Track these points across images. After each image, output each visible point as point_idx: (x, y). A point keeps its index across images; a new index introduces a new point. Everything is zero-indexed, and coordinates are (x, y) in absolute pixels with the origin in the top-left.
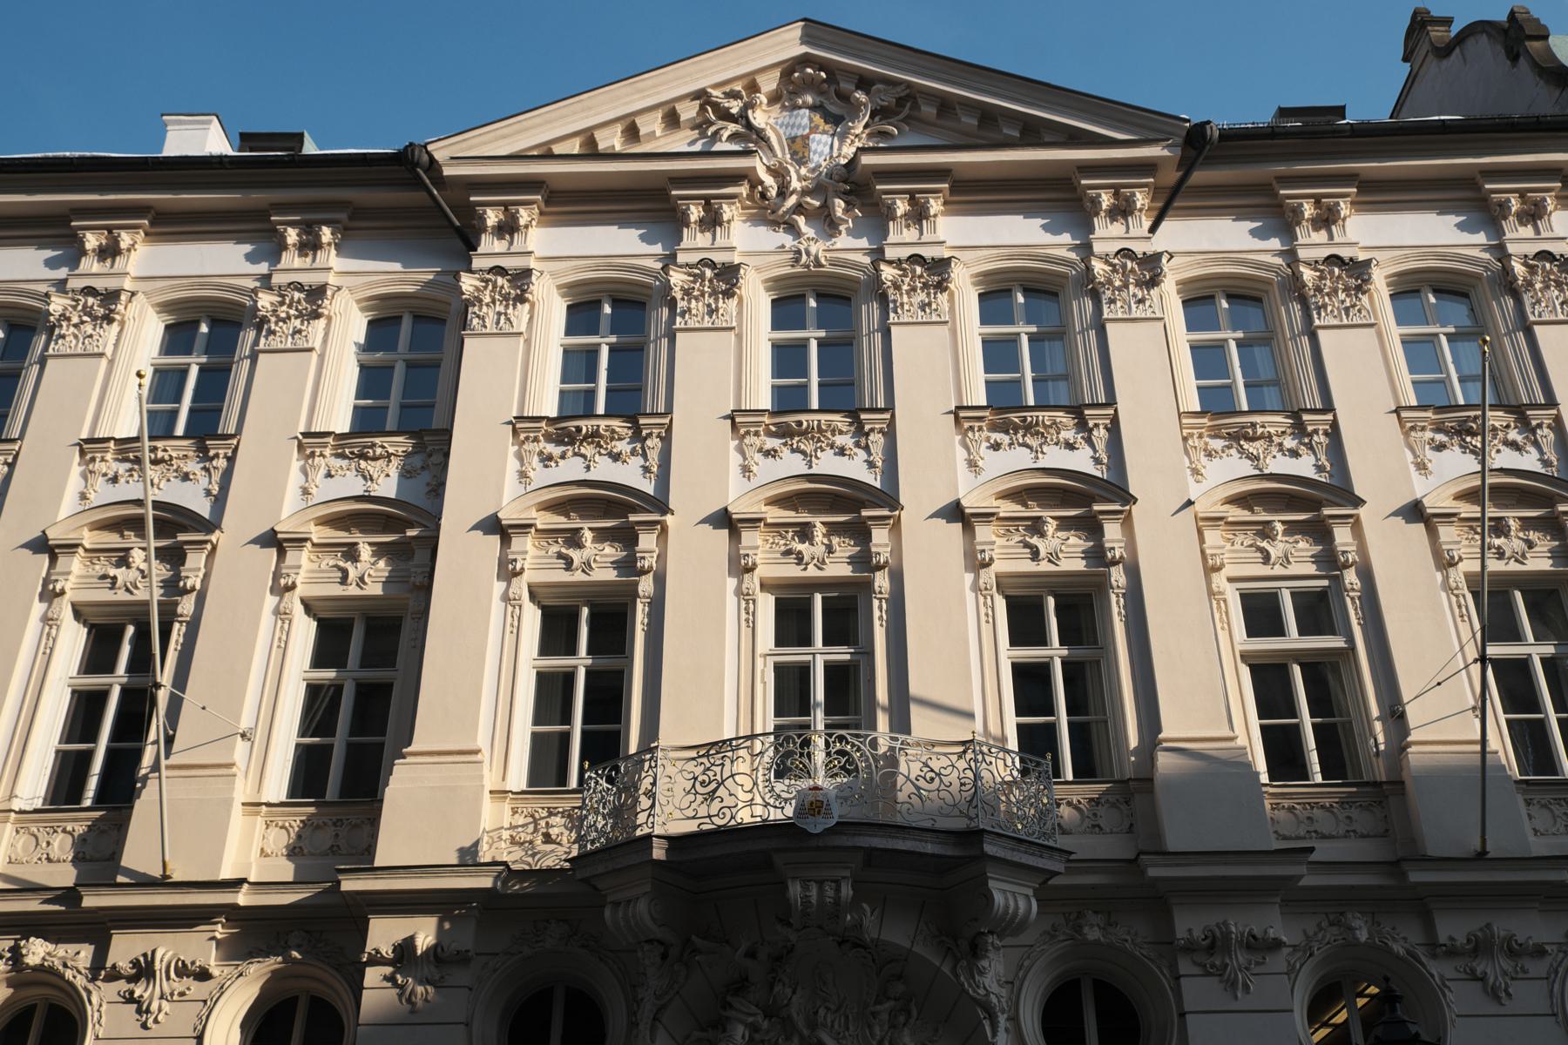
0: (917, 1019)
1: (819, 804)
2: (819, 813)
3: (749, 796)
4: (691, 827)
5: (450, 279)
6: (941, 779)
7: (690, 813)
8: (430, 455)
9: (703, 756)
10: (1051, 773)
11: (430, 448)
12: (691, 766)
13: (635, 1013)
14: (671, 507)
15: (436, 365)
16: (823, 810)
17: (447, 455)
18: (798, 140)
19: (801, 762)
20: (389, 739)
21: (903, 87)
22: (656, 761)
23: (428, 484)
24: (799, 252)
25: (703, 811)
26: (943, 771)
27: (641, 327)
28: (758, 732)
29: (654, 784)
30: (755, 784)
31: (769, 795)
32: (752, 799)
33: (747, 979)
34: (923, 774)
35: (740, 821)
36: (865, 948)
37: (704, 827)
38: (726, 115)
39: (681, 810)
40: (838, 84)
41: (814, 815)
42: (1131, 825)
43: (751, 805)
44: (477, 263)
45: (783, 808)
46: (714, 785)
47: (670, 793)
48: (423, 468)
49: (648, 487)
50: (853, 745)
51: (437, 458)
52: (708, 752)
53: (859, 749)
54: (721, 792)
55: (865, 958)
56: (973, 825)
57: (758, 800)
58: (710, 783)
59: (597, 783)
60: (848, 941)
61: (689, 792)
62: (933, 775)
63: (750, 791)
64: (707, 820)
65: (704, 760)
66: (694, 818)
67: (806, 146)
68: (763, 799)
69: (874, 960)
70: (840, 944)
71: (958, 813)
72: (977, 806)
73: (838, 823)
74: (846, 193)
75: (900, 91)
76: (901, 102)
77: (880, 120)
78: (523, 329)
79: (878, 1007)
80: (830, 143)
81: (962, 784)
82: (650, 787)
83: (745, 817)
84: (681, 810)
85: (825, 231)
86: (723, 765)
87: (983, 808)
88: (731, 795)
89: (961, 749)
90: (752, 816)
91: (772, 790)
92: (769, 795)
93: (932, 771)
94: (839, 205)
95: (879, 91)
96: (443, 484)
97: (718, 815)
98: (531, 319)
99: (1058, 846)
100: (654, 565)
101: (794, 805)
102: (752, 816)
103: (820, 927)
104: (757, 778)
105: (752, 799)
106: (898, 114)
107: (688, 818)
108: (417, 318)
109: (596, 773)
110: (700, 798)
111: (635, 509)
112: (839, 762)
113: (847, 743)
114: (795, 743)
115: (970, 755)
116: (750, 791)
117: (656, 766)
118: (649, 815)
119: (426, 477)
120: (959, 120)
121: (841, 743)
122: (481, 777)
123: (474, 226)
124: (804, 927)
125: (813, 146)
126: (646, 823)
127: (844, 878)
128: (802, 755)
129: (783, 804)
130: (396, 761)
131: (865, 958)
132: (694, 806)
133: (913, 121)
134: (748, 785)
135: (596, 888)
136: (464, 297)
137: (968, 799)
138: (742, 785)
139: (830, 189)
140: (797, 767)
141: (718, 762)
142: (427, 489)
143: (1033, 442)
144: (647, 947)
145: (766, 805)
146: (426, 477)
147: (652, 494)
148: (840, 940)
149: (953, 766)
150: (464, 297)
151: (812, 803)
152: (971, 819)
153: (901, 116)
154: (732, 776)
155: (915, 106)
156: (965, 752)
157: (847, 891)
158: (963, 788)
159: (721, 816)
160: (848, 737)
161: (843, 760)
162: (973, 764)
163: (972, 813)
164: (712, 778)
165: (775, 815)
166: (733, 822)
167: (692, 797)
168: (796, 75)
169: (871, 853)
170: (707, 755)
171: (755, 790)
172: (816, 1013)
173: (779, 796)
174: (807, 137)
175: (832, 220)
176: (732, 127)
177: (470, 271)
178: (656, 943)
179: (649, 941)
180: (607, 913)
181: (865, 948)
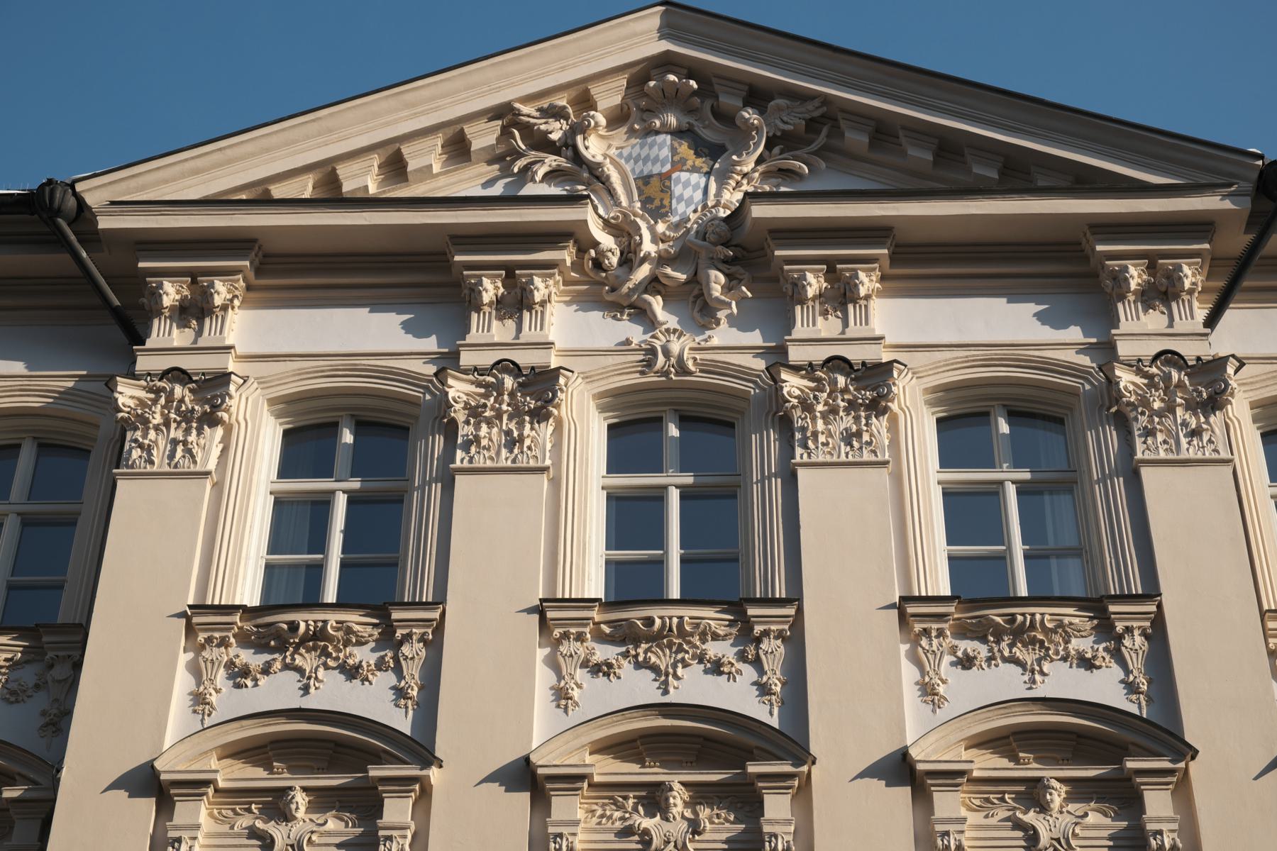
5: (98, 387)
8: (51, 666)
11: (50, 654)
14: (438, 754)
15: (70, 522)
17: (78, 666)
18: (655, 181)
21: (816, 103)
23: (44, 713)
24: (652, 351)
27: (399, 466)
38: (542, 144)
40: (717, 97)
44: (144, 363)
48: (37, 687)
49: (403, 722)
51: (60, 672)
67: (666, 190)
74: (727, 261)
75: (812, 110)
76: (813, 125)
78: (212, 465)
80: (702, 185)
85: (693, 318)
94: (717, 281)
95: (779, 109)
96: (67, 714)
98: (225, 451)
106: (810, 143)
108: (45, 447)
111: (379, 758)
119: (40, 701)
120: (904, 153)
123: (142, 307)
125: (677, 190)
133: (832, 154)
136: (120, 415)
139: (703, 254)
142: (42, 721)
143: (1028, 656)
146: (40, 701)
147: (408, 733)
150: (120, 415)
153: (814, 147)
155: (836, 132)
168: (652, 83)
177: (132, 375)
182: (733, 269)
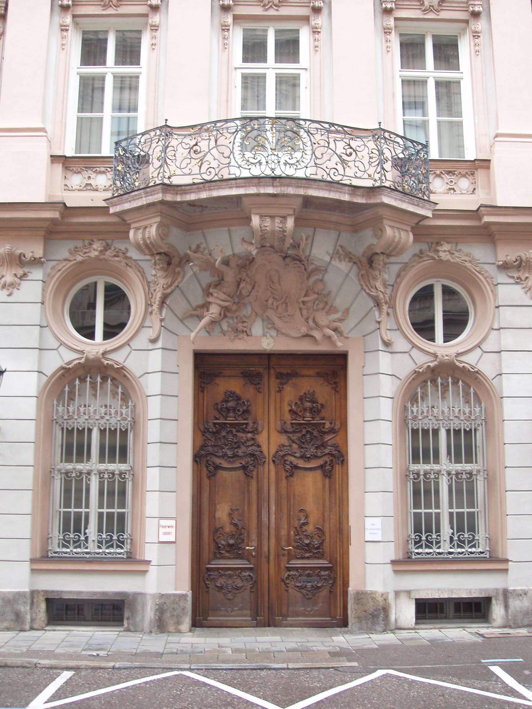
6: (356, 153)
7: (187, 171)
12: (187, 140)
26: (358, 149)
32: (229, 163)
39: (181, 169)
45: (250, 169)
57: (233, 163)
58: (200, 152)
62: (351, 150)
63: (229, 157)
66: (190, 174)
68: (237, 162)
69: (305, 270)
71: (367, 176)
79: (306, 299)
81: (370, 158)
84: (181, 169)
86: (210, 139)
88: (215, 159)
93: (351, 148)
97: (206, 173)
102: (229, 174)
104: (233, 148)
105: (229, 163)
107: (185, 175)
116: (229, 157)
126: (158, 177)
127: (289, 215)
132: (189, 166)
134: (227, 153)
135: (124, 220)
138: (223, 153)
145: (240, 166)
148: (284, 255)
149: (365, 145)
152: (375, 180)
157: (290, 223)
158: (371, 160)
159: (209, 174)
169: (308, 201)
171: (232, 156)
172: (267, 301)
178: (163, 255)
180: (131, 233)
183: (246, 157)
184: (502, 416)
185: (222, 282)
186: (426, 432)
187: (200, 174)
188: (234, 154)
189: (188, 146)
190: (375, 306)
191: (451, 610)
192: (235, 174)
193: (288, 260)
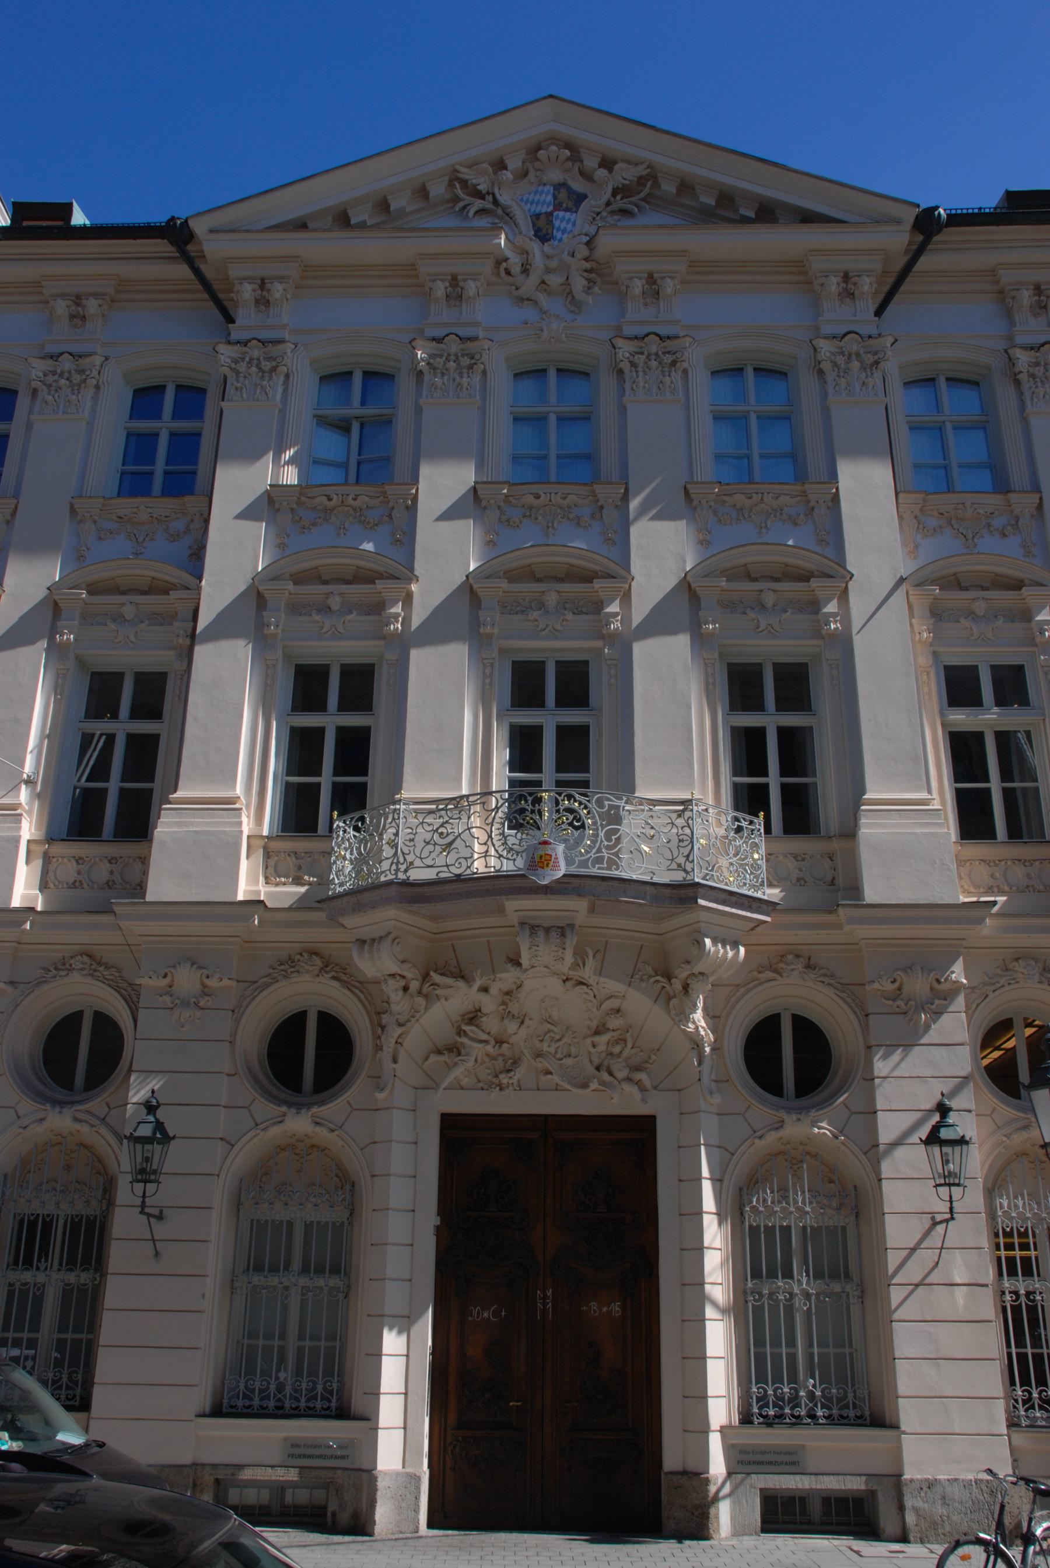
0: (632, 1048)
1: (548, 857)
2: (547, 865)
3: (484, 848)
4: (430, 874)
9: (442, 809)
10: (762, 831)
13: (379, 1038)
14: (416, 573)
16: (551, 863)
18: (543, 217)
19: (532, 819)
20: (157, 786)
22: (399, 814)
23: (190, 547)
25: (439, 861)
28: (494, 790)
29: (396, 834)
30: (490, 837)
31: (502, 847)
32: (487, 851)
33: (480, 1010)
34: (644, 831)
35: (475, 871)
36: (587, 985)
37: (442, 875)
40: (582, 161)
41: (543, 868)
42: (834, 878)
43: (485, 856)
45: (514, 860)
46: (451, 838)
47: (412, 844)
50: (580, 803)
52: (446, 806)
53: (586, 807)
54: (458, 843)
55: (587, 993)
56: (689, 878)
57: (492, 852)
58: (448, 835)
59: (345, 831)
60: (571, 979)
61: (428, 843)
63: (485, 844)
64: (445, 869)
65: (443, 813)
67: (550, 223)
68: (497, 851)
69: (595, 997)
70: (564, 981)
72: (693, 861)
73: (565, 875)
77: (622, 198)
81: (680, 841)
82: (393, 838)
83: (479, 866)
84: (421, 859)
87: (699, 863)
89: (681, 808)
90: (486, 867)
91: (505, 843)
92: (502, 847)
93: (652, 828)
99: (765, 898)
100: (400, 628)
101: (524, 857)
102: (486, 867)
103: (546, 967)
104: (491, 832)
105: (487, 851)
106: (639, 193)
107: (429, 867)
109: (345, 822)
110: (438, 849)
112: (567, 819)
113: (575, 801)
114: (526, 801)
115: (687, 814)
116: (485, 844)
117: (399, 818)
118: (392, 863)
121: (569, 800)
122: (241, 823)
123: (232, 300)
124: (533, 967)
125: (557, 223)
126: (390, 870)
128: (533, 812)
129: (515, 856)
130: (164, 806)
131: (587, 993)
132: (433, 855)
134: (484, 837)
137: (685, 854)
138: (478, 838)
140: (528, 823)
141: (455, 817)
144: (391, 982)
145: (500, 856)
148: (565, 978)
151: (541, 857)
153: (642, 195)
154: (469, 829)
155: (656, 184)
156: (683, 811)
158: (681, 844)
160: (577, 796)
161: (571, 817)
162: (690, 822)
163: (689, 867)
164: (450, 831)
165: (507, 866)
166: (468, 872)
167: (430, 848)
170: (445, 809)
171: (489, 843)
173: (511, 849)
174: (551, 214)
175: (573, 297)
176: (479, 204)
178: (398, 978)
179: (392, 975)
181: (587, 985)
182: (593, 275)
183: (509, 843)
184: (883, 1210)
185: (479, 1014)
186: (770, 1231)
187: (447, 866)
188: (492, 839)
189: (430, 828)
190: (693, 1048)
191: (816, 1509)
192: (494, 867)
193: (569, 984)
